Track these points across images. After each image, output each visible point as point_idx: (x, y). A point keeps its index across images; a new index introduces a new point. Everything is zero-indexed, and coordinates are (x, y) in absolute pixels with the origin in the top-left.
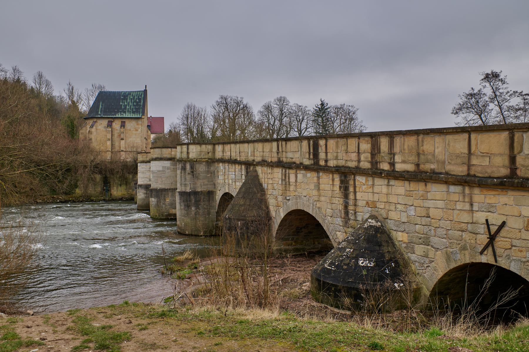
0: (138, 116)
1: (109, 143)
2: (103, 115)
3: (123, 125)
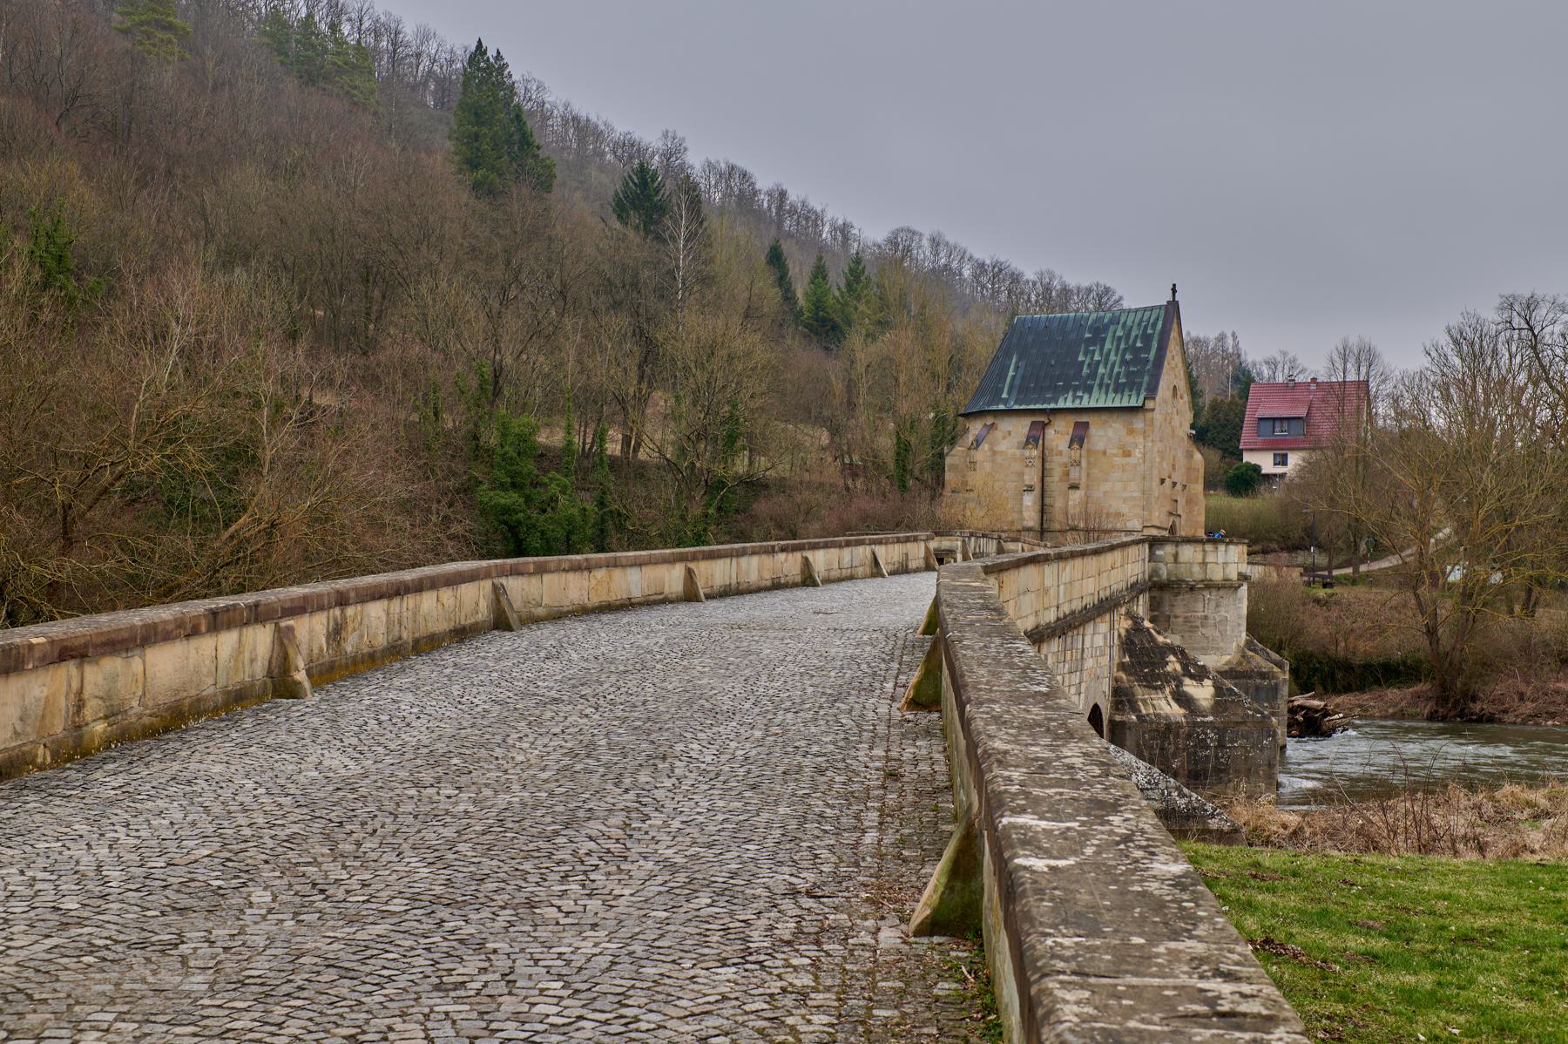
0: (1133, 403)
1: (1030, 500)
2: (1015, 403)
3: (1079, 437)
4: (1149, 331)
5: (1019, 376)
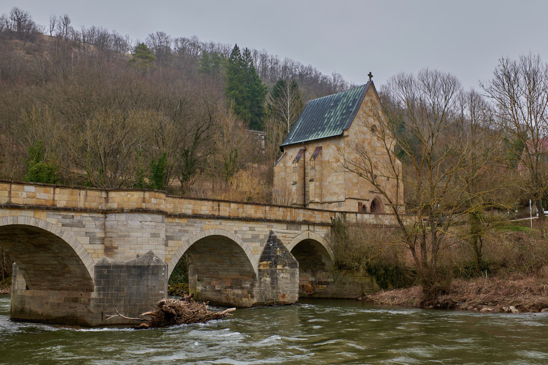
0: (338, 134)
5: (299, 129)
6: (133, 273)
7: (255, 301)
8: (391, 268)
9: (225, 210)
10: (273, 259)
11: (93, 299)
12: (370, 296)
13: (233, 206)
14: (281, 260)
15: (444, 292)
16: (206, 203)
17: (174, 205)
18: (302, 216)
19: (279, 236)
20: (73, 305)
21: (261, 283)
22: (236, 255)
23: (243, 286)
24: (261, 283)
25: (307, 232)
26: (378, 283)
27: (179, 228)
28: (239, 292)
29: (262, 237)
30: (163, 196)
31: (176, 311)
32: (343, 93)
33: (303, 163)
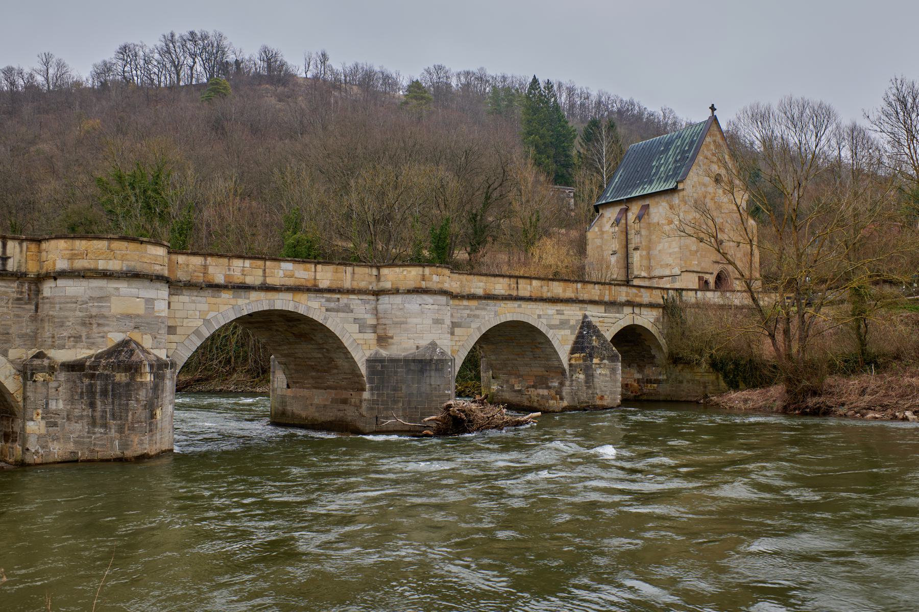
0: (671, 187)
4: (695, 138)
6: (412, 368)
7: (565, 403)
8: (742, 362)
9: (525, 289)
10: (588, 351)
11: (365, 400)
12: (715, 398)
13: (535, 283)
14: (598, 352)
15: (815, 393)
16: (501, 280)
17: (461, 283)
18: (624, 294)
19: (595, 321)
20: (342, 407)
21: (572, 381)
22: (539, 346)
23: (550, 384)
24: (572, 381)
25: (632, 316)
26: (725, 382)
27: (468, 312)
28: (544, 392)
29: (572, 322)
30: (447, 272)
31: (466, 415)
32: (677, 133)
33: (624, 226)
